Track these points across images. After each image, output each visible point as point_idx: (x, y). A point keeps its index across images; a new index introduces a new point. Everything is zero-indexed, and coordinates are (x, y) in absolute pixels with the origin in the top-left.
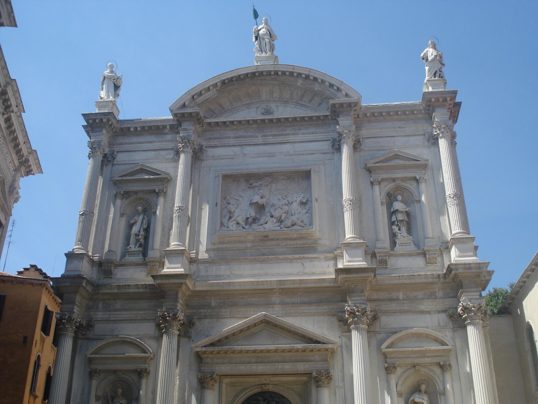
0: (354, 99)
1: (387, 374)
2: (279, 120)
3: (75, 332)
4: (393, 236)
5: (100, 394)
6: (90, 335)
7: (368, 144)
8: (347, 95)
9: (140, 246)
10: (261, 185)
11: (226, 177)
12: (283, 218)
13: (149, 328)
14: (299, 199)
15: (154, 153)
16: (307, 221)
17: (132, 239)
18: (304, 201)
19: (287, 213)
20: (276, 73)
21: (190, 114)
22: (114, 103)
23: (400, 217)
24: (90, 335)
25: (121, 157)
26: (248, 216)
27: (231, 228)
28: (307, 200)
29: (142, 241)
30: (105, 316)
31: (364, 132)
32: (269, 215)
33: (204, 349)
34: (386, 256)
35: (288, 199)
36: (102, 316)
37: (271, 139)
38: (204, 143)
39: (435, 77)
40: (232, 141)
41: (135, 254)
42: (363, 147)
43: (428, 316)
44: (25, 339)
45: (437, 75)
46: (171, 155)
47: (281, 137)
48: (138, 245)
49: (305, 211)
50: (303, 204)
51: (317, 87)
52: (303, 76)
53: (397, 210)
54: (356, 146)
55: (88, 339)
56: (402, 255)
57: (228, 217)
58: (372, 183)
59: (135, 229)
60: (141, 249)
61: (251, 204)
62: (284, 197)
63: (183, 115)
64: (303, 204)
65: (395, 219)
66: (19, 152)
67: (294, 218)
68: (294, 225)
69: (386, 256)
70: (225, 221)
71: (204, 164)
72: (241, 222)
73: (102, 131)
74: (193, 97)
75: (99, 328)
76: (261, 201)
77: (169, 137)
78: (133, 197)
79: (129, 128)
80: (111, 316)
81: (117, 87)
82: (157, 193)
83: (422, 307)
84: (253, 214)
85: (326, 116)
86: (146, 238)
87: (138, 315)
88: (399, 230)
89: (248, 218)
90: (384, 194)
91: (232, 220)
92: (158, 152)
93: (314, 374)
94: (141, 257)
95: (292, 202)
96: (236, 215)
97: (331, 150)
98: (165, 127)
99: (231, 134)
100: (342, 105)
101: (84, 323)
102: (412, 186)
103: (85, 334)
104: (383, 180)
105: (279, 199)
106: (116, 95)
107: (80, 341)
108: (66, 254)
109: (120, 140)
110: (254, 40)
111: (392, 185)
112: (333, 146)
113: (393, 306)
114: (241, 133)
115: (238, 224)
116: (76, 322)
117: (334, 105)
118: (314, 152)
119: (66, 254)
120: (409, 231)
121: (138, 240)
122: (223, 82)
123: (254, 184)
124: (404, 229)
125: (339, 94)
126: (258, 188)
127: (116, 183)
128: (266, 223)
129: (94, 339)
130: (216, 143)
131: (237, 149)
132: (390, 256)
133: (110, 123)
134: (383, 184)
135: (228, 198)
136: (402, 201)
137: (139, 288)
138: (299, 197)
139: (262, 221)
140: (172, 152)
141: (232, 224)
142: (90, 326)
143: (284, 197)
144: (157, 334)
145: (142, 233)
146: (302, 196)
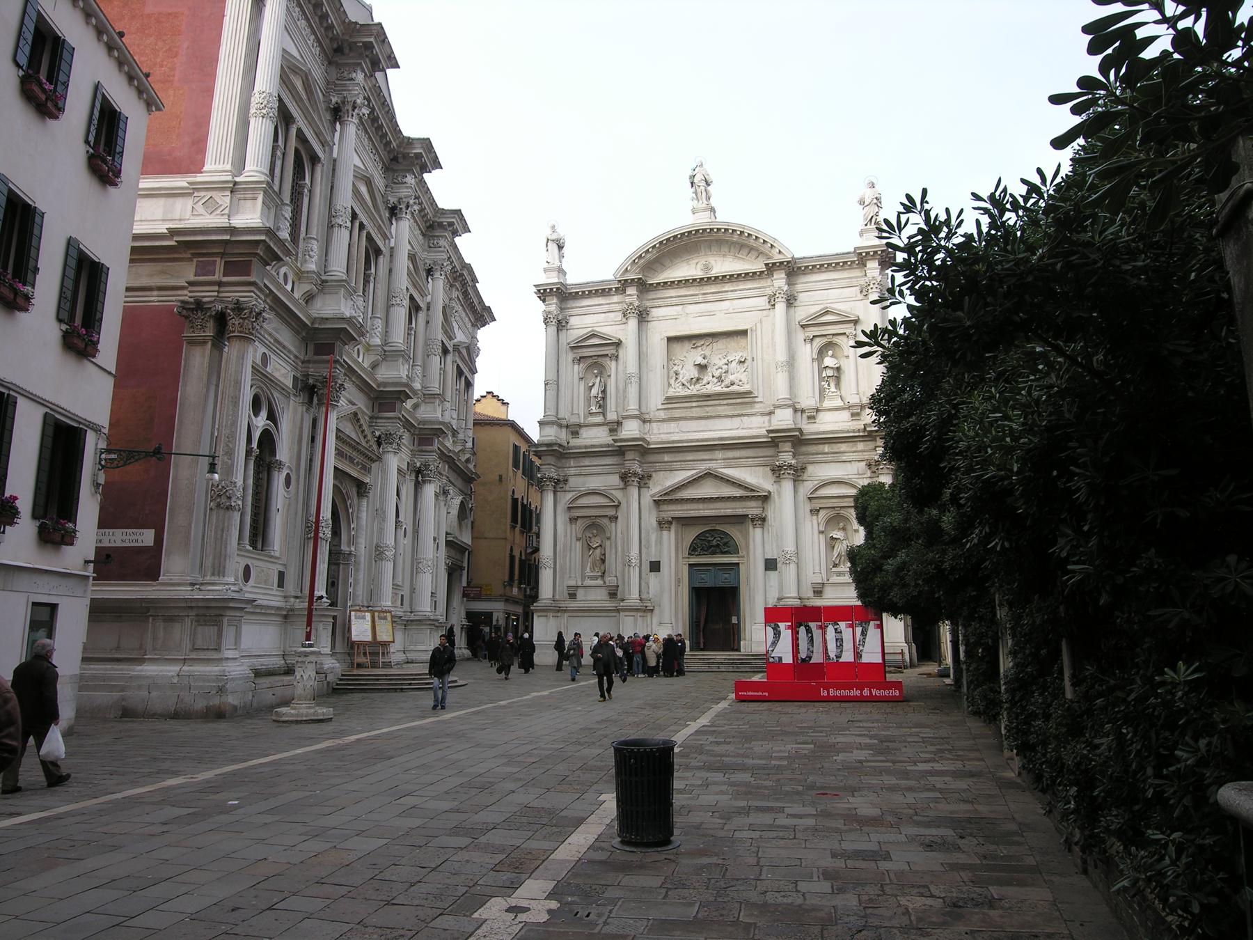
0: (788, 257)
2: (717, 277)
4: (822, 392)
7: (802, 297)
11: (670, 340)
13: (615, 480)
16: (745, 380)
17: (593, 401)
19: (726, 372)
20: (712, 229)
22: (561, 271)
23: (830, 373)
25: (574, 321)
31: (799, 287)
37: (710, 297)
38: (648, 304)
40: (674, 301)
44: (501, 477)
46: (619, 316)
51: (752, 242)
54: (791, 301)
56: (829, 410)
59: (594, 392)
66: (474, 311)
67: (731, 378)
70: (672, 381)
71: (651, 325)
75: (573, 482)
76: (704, 362)
77: (616, 299)
78: (590, 361)
81: (560, 247)
86: (604, 398)
90: (815, 351)
96: (681, 377)
98: (610, 289)
99: (672, 293)
106: (561, 257)
109: (571, 304)
111: (825, 340)
114: (683, 292)
117: (767, 265)
120: (838, 385)
122: (661, 243)
124: (832, 385)
127: (572, 348)
132: (818, 410)
134: (817, 340)
136: (832, 356)
138: (737, 356)
139: (705, 381)
142: (566, 481)
144: (622, 485)
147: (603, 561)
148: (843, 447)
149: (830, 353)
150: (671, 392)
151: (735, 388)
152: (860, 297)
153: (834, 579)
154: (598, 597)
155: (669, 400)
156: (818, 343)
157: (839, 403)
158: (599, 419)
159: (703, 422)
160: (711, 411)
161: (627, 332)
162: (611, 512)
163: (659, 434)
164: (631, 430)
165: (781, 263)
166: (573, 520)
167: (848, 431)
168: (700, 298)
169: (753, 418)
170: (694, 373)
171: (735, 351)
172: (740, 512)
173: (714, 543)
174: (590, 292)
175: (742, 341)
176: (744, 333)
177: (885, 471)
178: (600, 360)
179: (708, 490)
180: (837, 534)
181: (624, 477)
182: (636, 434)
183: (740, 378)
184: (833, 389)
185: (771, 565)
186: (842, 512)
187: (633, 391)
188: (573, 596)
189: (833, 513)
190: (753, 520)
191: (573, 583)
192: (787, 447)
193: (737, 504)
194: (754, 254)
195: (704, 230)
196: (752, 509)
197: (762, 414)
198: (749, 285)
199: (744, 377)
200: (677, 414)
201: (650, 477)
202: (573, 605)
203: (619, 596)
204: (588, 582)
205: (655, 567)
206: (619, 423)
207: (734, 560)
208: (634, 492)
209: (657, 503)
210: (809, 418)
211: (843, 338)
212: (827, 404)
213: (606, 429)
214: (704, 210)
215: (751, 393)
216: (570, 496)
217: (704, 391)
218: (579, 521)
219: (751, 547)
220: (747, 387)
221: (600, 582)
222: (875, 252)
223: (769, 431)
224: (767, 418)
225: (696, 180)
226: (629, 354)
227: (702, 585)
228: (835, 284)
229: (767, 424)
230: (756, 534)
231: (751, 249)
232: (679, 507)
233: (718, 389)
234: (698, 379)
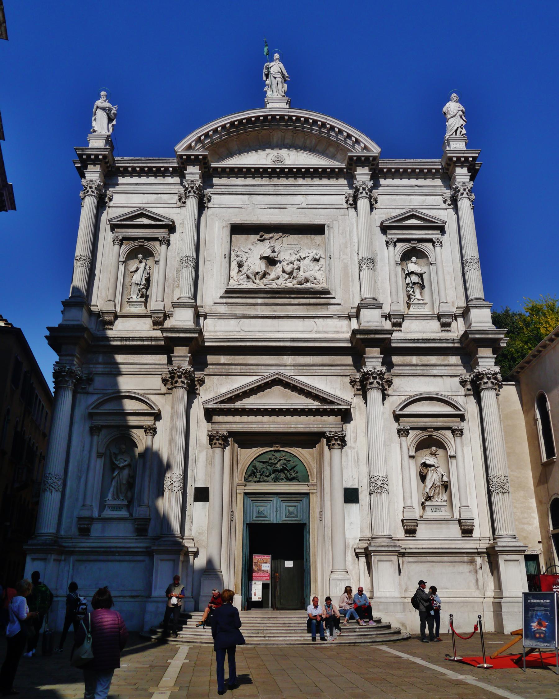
1: (399, 435)
2: (291, 169)
3: (75, 385)
5: (102, 450)
6: (91, 389)
8: (366, 148)
9: (142, 296)
10: (272, 238)
12: (295, 274)
14: (311, 255)
15: (155, 196)
18: (317, 257)
20: (290, 117)
21: (197, 156)
23: (415, 279)
24: (91, 389)
25: (118, 199)
26: (259, 271)
27: (242, 283)
28: (320, 257)
29: (144, 290)
30: (106, 370)
32: (281, 269)
33: (215, 406)
34: (400, 318)
35: (300, 254)
36: (103, 369)
39: (456, 134)
41: (137, 305)
42: (378, 205)
43: (439, 379)
45: (458, 132)
47: (293, 188)
48: (140, 295)
49: (318, 268)
50: (317, 260)
52: (320, 123)
53: (412, 273)
55: (88, 393)
57: (237, 270)
58: (387, 242)
59: (137, 278)
60: (143, 300)
61: (262, 258)
62: (296, 253)
63: (189, 156)
64: (317, 260)
65: (410, 282)
67: (307, 275)
68: (306, 283)
69: (400, 318)
70: (234, 273)
71: (210, 212)
72: (251, 276)
73: (97, 168)
74: (200, 137)
76: (272, 255)
78: (133, 244)
79: (126, 168)
80: (113, 370)
82: (160, 241)
83: (435, 372)
84: (264, 269)
85: (341, 169)
87: (143, 370)
88: (413, 291)
89: (258, 273)
91: (241, 273)
92: (159, 195)
93: (328, 434)
94: (143, 307)
95: (304, 258)
97: (345, 206)
98: (167, 169)
100: (359, 158)
101: (84, 377)
102: (427, 247)
103: (85, 388)
104: (399, 240)
105: (291, 254)
107: (78, 395)
108: (63, 303)
110: (264, 78)
112: (347, 202)
113: (406, 370)
114: (250, 181)
115: (248, 277)
116: (76, 375)
117: (351, 158)
118: (328, 206)
119: (63, 303)
121: (139, 291)
123: (263, 238)
124: (417, 292)
125: (357, 146)
126: (268, 241)
128: (278, 279)
129: (93, 394)
130: (223, 190)
131: (246, 197)
133: (107, 160)
134: (399, 244)
135: (236, 249)
137: (144, 341)
138: (312, 253)
139: (273, 275)
140: (176, 197)
141: (241, 277)
142: (90, 380)
143: (296, 253)
144: (164, 389)
145: (144, 282)
146: (314, 252)
147: (131, 485)
148: (433, 360)
149: (414, 259)
150: (233, 284)
151: (308, 285)
152: (444, 206)
153: (429, 514)
154: (120, 534)
155: (230, 292)
156: (401, 247)
157: (426, 311)
158: (140, 309)
159: (269, 321)
160: (279, 311)
161: (184, 216)
162: (148, 421)
163: (215, 330)
164: (183, 318)
165: (367, 158)
166: (94, 431)
167: (441, 340)
168: (271, 190)
169: (329, 321)
170: (261, 266)
171: (307, 246)
172: (314, 428)
173: (279, 466)
174: (142, 168)
175: (318, 239)
176: (318, 230)
177: (490, 385)
178: (147, 244)
179: (275, 398)
180: (430, 460)
181: (170, 381)
182: (190, 324)
183: (315, 275)
184: (418, 296)
185: (351, 496)
186: (435, 434)
187: (187, 275)
188: (84, 531)
189: (424, 435)
190: (329, 440)
191: (86, 513)
192: (375, 352)
193: (311, 419)
194: (332, 150)
195: (282, 117)
196: (328, 424)
197: (340, 317)
198: (325, 181)
199: (318, 275)
200: (239, 310)
201: (202, 382)
202: (85, 544)
203: (151, 533)
204: (108, 513)
205: (202, 495)
206: (166, 316)
207: (302, 488)
208: (181, 394)
209: (209, 414)
210: (394, 325)
211: (430, 245)
212: (413, 311)
213: (149, 322)
214: (279, 101)
215: (328, 292)
216: (92, 399)
217: (274, 286)
218: (103, 432)
219: (327, 473)
220: (323, 285)
221: (124, 513)
222: (466, 158)
223: (355, 332)
224: (346, 322)
225: (272, 70)
226: (182, 242)
227: (261, 520)
228: (416, 190)
229: (345, 329)
230: (333, 457)
231: (330, 143)
232: (237, 418)
233: (290, 284)
234: (265, 275)
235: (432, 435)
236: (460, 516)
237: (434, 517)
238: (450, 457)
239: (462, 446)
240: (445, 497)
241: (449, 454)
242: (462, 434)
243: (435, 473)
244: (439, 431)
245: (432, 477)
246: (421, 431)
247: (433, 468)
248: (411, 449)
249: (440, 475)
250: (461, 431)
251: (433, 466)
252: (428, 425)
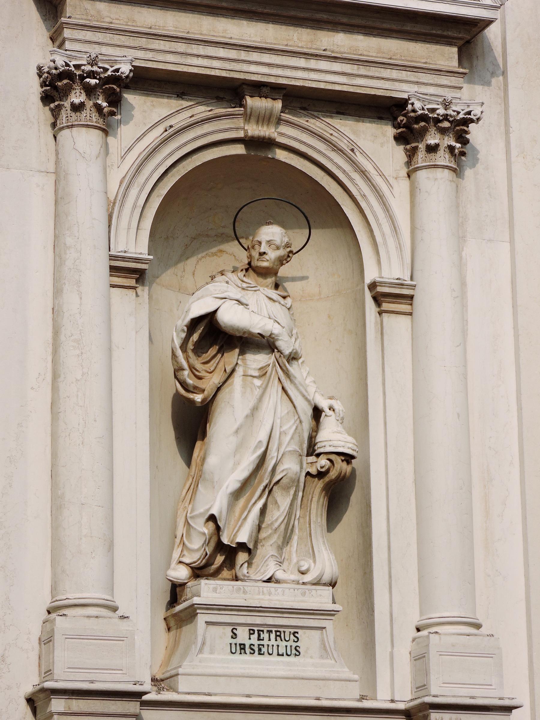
189: (219, 129)
235: (268, 144)
236: (422, 687)
237: (250, 687)
238: (378, 299)
239: (460, 238)
240: (325, 561)
241: (371, 275)
242: (461, 153)
243: (274, 392)
244: (315, 124)
245: (251, 418)
246: (202, 110)
247: (256, 360)
248: (127, 217)
249: (307, 412)
250: (460, 127)
251: (266, 344)
252: (255, 69)
